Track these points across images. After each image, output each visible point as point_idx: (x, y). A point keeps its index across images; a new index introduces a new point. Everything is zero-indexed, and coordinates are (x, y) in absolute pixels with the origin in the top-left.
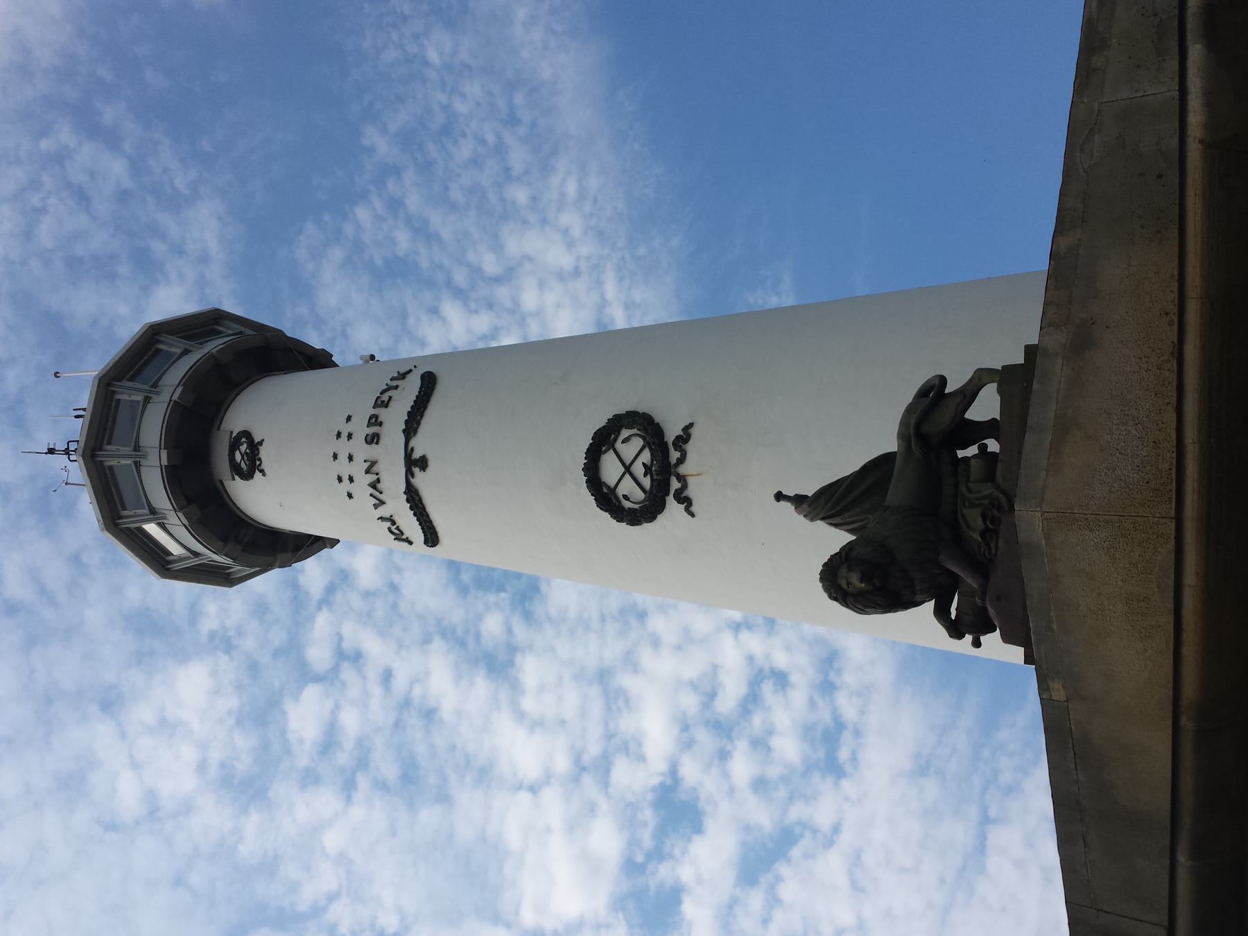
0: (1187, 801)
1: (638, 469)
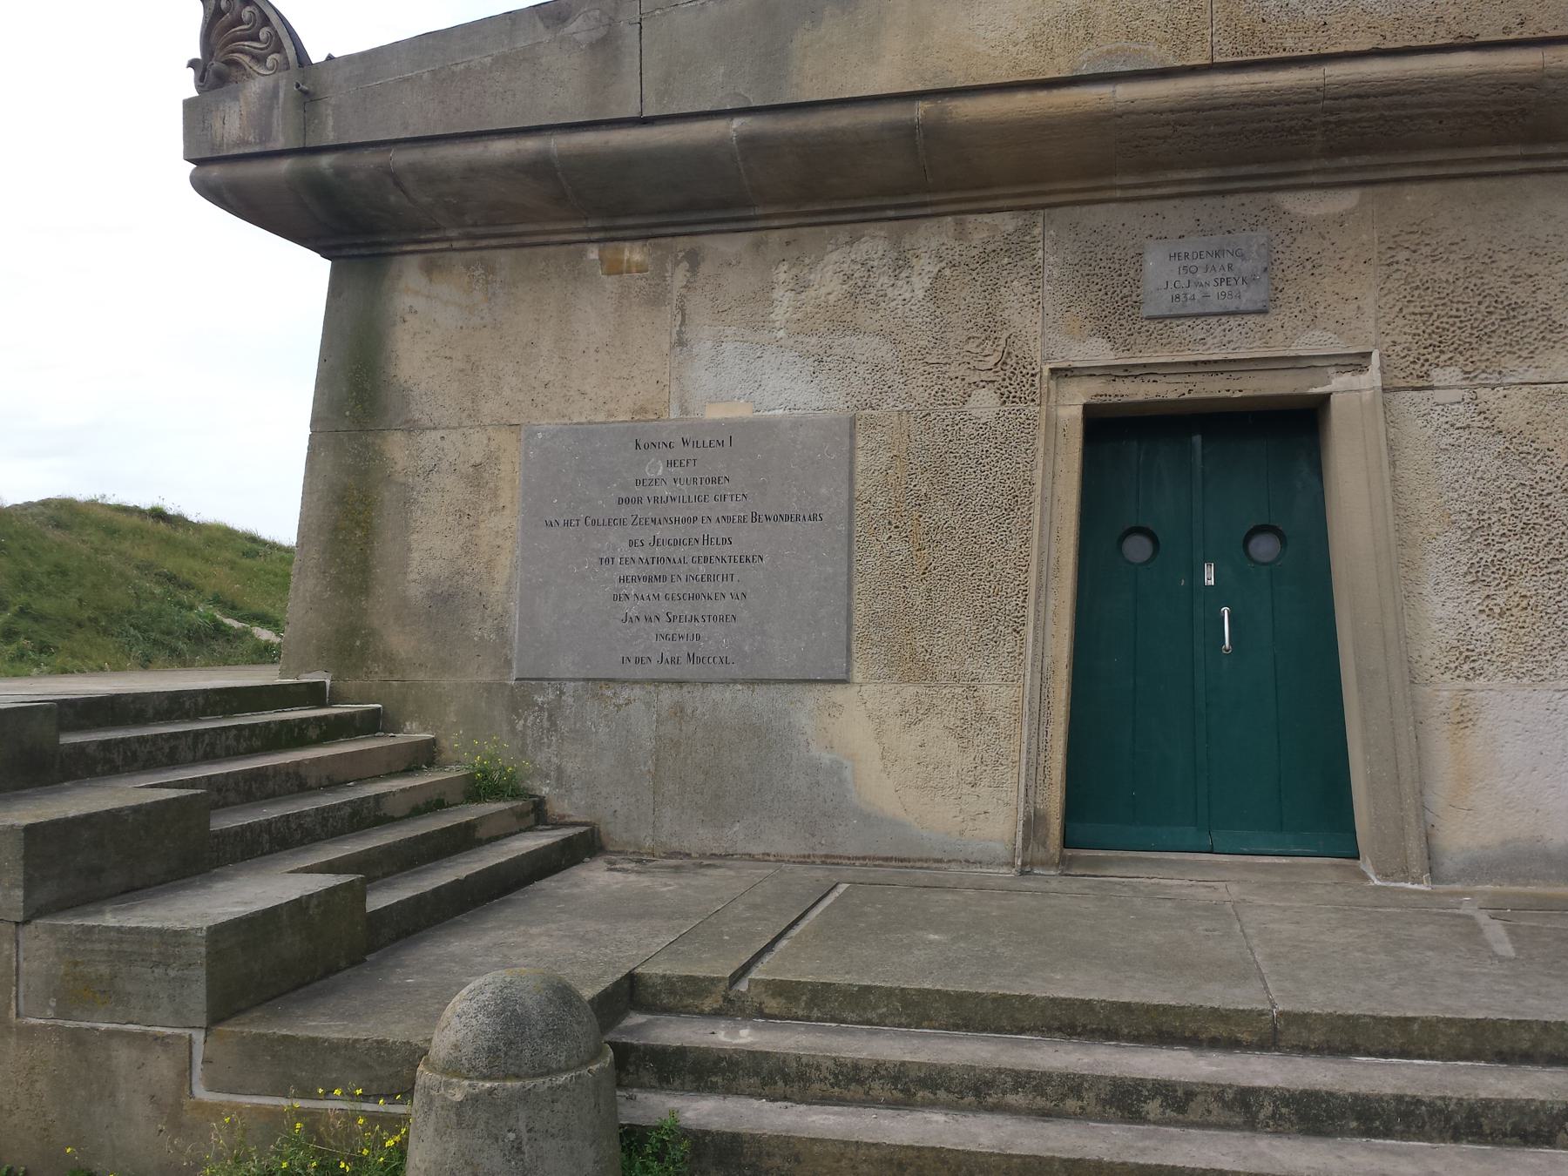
0: (816, 122)
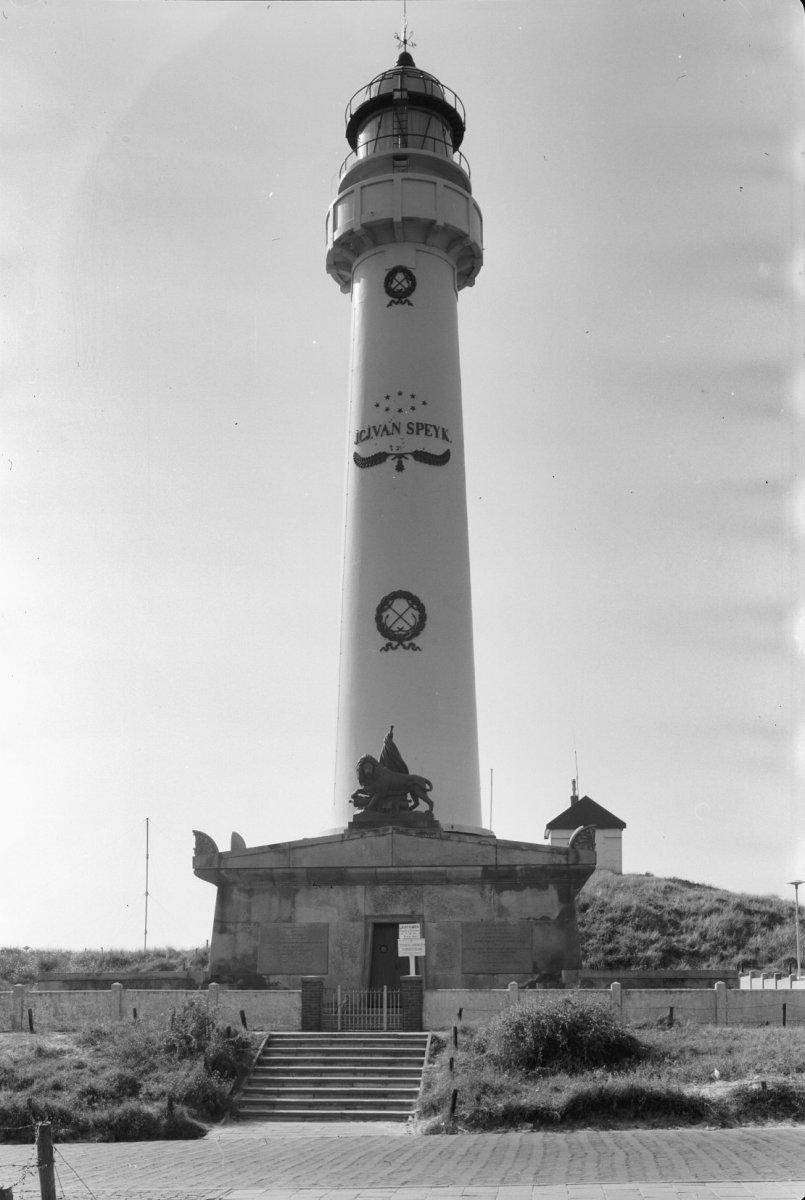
1: (401, 624)
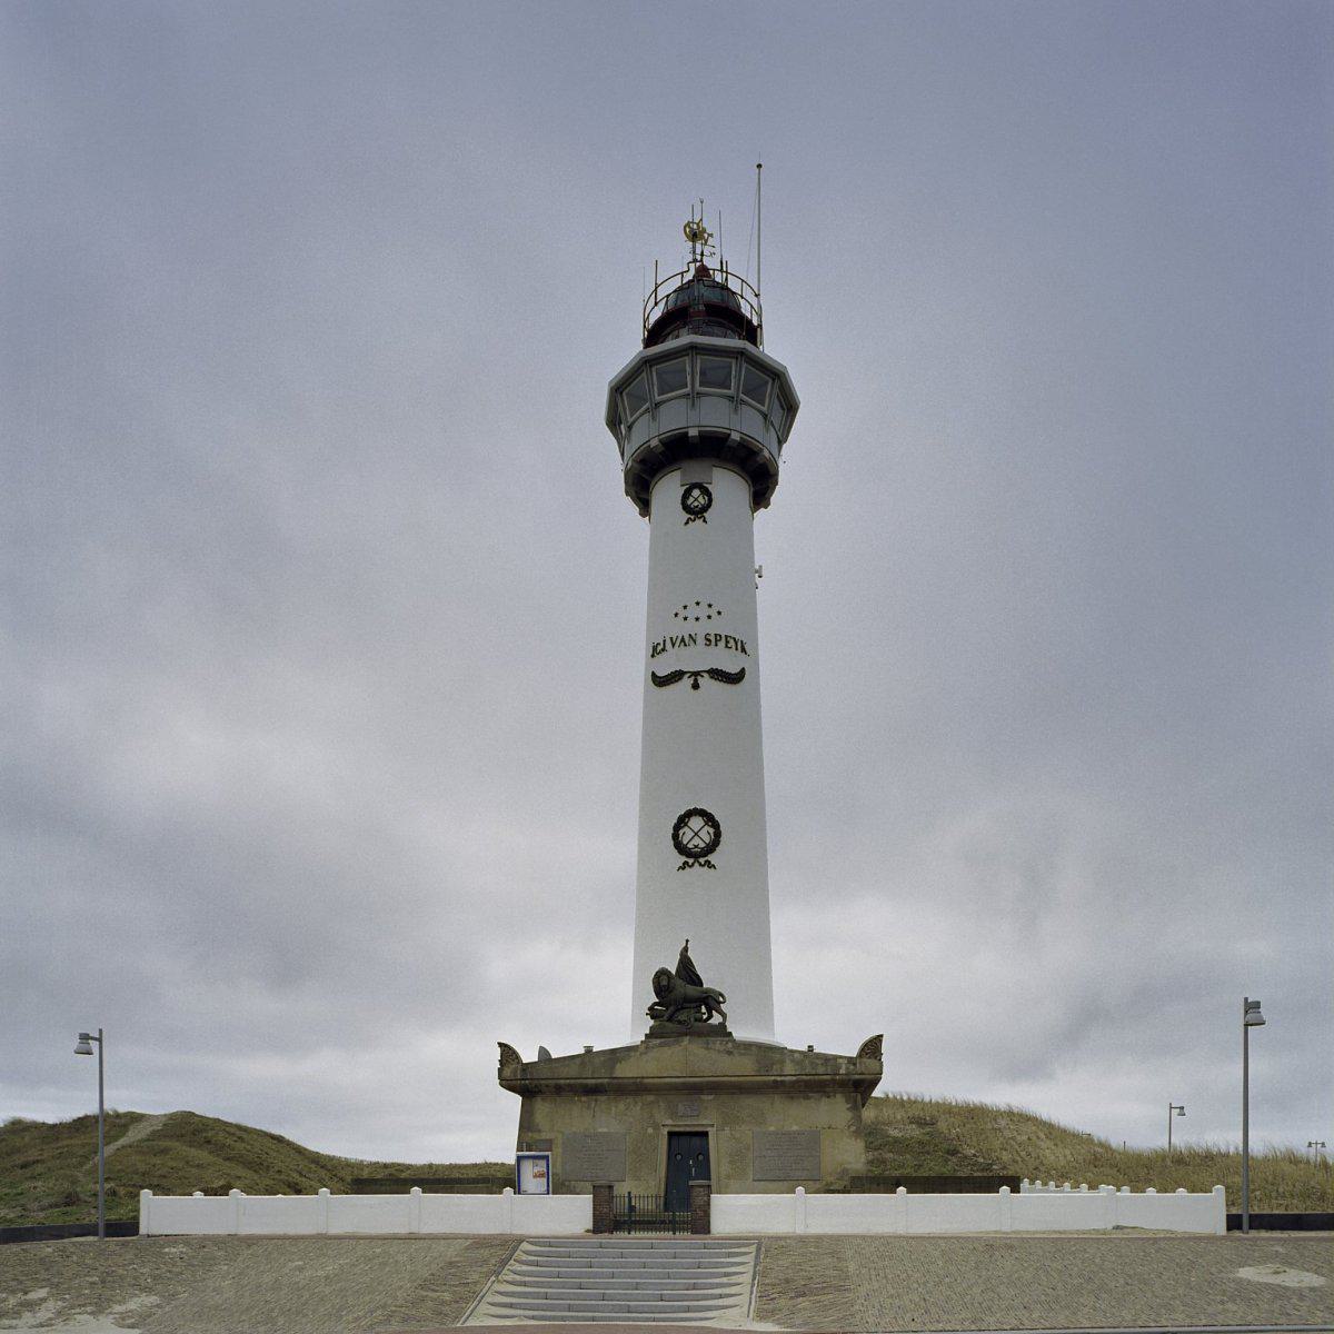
1: (696, 841)
